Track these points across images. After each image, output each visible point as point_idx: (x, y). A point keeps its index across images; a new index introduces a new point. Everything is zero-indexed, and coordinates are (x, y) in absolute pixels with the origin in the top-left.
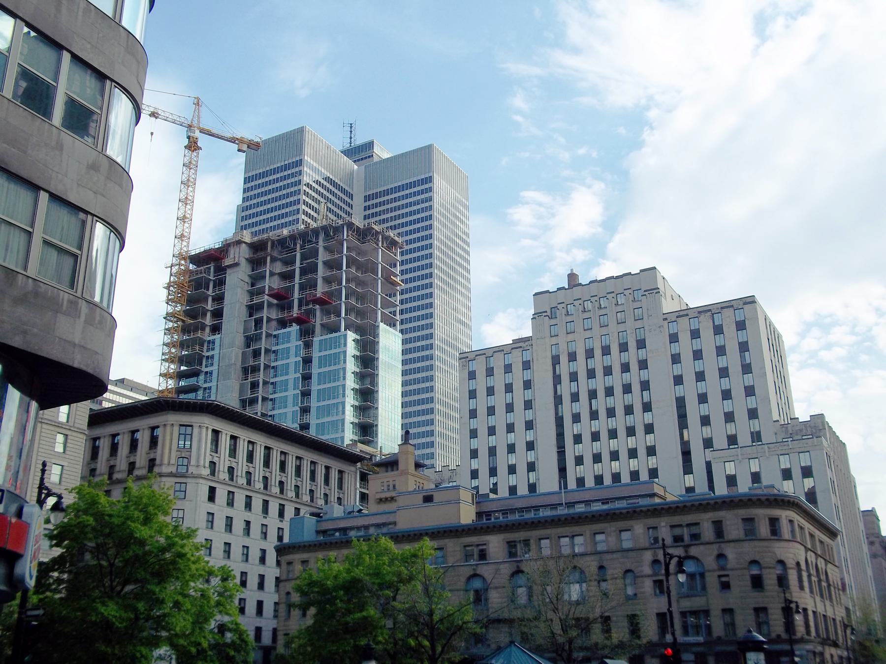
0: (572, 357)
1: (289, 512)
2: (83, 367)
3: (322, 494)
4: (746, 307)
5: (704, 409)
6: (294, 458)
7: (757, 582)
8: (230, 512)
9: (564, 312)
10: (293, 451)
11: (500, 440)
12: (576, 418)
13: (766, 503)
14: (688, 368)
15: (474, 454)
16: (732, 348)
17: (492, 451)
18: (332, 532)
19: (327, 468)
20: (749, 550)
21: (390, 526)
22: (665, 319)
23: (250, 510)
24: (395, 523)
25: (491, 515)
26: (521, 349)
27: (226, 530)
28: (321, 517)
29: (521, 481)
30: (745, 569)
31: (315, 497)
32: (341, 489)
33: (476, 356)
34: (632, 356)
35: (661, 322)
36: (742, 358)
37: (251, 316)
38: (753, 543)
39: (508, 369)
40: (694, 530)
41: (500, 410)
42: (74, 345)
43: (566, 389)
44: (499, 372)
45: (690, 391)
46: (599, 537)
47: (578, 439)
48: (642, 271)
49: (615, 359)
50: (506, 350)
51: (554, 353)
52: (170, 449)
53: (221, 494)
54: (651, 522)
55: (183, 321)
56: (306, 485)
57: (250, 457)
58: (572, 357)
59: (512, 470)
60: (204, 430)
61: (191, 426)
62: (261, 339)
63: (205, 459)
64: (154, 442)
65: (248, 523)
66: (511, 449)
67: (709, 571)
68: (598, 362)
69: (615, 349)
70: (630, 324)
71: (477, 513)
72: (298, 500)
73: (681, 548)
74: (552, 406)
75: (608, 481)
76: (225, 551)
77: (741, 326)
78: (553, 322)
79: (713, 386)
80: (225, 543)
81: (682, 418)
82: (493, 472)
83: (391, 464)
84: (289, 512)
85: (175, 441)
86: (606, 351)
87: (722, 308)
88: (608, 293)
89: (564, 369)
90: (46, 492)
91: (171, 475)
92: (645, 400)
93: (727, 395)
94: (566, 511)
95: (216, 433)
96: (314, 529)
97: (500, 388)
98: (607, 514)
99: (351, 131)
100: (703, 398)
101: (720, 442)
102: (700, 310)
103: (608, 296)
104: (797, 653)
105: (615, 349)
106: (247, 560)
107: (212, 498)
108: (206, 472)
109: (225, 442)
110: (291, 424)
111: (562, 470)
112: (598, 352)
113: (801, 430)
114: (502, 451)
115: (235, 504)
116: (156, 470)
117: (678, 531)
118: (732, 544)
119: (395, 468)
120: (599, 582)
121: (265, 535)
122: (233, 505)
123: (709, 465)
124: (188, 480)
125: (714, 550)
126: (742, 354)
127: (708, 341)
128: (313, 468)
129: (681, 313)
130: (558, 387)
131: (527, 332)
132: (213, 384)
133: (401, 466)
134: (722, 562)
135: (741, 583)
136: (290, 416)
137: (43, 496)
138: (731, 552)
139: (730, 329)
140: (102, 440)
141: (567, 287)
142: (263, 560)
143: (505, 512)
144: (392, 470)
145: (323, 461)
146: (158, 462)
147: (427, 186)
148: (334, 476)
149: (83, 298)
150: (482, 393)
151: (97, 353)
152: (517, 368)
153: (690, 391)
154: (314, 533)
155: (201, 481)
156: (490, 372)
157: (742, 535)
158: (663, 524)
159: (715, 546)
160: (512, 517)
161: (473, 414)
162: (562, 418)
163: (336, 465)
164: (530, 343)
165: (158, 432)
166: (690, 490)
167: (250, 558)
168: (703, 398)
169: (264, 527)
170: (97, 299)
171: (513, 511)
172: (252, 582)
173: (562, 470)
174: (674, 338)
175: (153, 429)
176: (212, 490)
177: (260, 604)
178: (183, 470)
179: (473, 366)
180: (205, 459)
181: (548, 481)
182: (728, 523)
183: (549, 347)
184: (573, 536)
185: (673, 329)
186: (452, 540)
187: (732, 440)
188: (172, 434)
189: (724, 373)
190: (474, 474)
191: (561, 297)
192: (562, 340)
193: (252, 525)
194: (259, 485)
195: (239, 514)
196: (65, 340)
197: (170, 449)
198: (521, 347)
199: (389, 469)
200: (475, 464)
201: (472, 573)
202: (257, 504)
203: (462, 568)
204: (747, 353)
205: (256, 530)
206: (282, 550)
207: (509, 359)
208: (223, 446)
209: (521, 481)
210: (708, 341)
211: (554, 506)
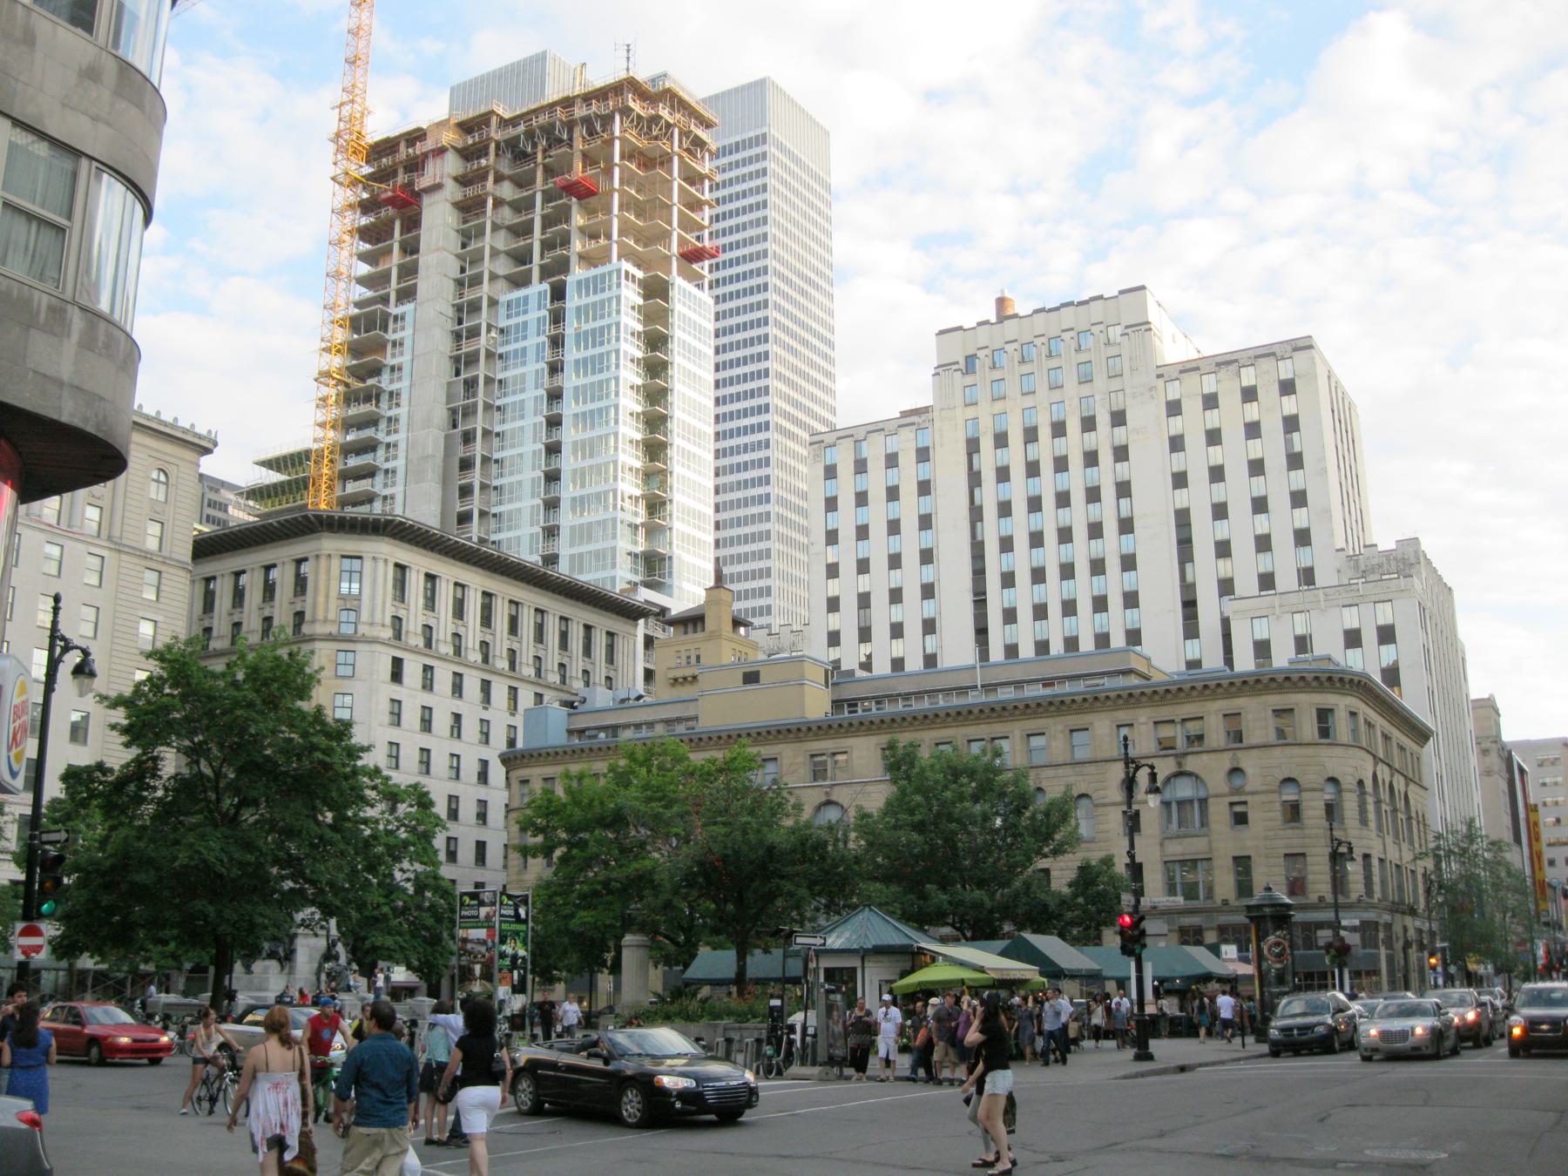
0: (1001, 440)
1: (526, 698)
2: (77, 422)
4: (1298, 356)
5: (1222, 530)
6: (532, 611)
7: (1294, 812)
9: (988, 362)
10: (531, 598)
11: (878, 582)
12: (1006, 544)
13: (1315, 684)
16: (1272, 428)
17: (864, 601)
18: (593, 733)
19: (588, 628)
20: (1284, 761)
21: (690, 724)
22: (1160, 376)
23: (461, 696)
24: (696, 718)
25: (856, 705)
26: (914, 428)
28: (575, 708)
29: (911, 650)
30: (1274, 792)
31: (568, 675)
33: (839, 438)
34: (1103, 439)
36: (1289, 443)
37: (458, 373)
38: (1287, 750)
39: (892, 460)
40: (1193, 728)
41: (878, 530)
42: (60, 383)
43: (989, 495)
44: (876, 465)
45: (1198, 497)
47: (1008, 580)
48: (1121, 292)
49: (1074, 445)
50: (892, 426)
51: (970, 434)
52: (327, 596)
53: (412, 670)
54: (1123, 716)
55: (347, 385)
56: (553, 657)
57: (459, 611)
58: (1001, 440)
59: (897, 631)
60: (381, 564)
61: (360, 558)
62: (475, 412)
63: (383, 612)
64: (301, 584)
65: (457, 717)
66: (896, 596)
67: (1217, 796)
68: (1045, 450)
69: (1073, 426)
70: (1100, 382)
71: (833, 702)
72: (540, 681)
73: (1171, 759)
75: (1057, 648)
76: (421, 762)
78: (969, 380)
79: (1238, 488)
80: (422, 750)
81: (1185, 544)
82: (865, 635)
83: (693, 621)
84: (526, 698)
85: (334, 583)
86: (1059, 429)
87: (1257, 357)
88: (1063, 331)
89: (987, 460)
90: (62, 644)
91: (330, 638)
92: (1124, 514)
93: (1260, 505)
94: (983, 699)
95: (401, 568)
96: (565, 727)
97: (877, 494)
98: (1051, 703)
99: (628, 58)
100: (1220, 511)
101: (1246, 584)
102: (1219, 360)
104: (1344, 923)
105: (1073, 426)
106: (458, 777)
107: (397, 676)
108: (387, 633)
109: (416, 583)
110: (530, 556)
111: (982, 632)
112: (1045, 433)
113: (1380, 566)
114: (880, 600)
116: (306, 629)
117: (1166, 732)
118: (1255, 752)
121: (486, 737)
122: (431, 689)
123: (1226, 623)
124: (359, 647)
125: (1225, 762)
126: (1289, 436)
128: (564, 629)
129: (1189, 366)
130: (977, 491)
132: (398, 490)
133: (710, 623)
134: (1237, 782)
135: (1264, 816)
137: (58, 650)
138: (1251, 763)
140: (219, 581)
141: (993, 320)
142: (483, 777)
143: (879, 701)
144: (695, 631)
145: (581, 615)
146: (308, 617)
148: (600, 641)
149: (74, 303)
150: (846, 501)
151: (101, 399)
152: (907, 459)
153: (1198, 497)
154: (565, 734)
155: (378, 648)
156: (861, 467)
157: (1272, 737)
158: (1142, 720)
159: (1229, 754)
160: (889, 708)
162: (982, 543)
163: (603, 622)
164: (930, 416)
166: (1194, 664)
167: (462, 774)
168: (1220, 511)
169: (485, 724)
170: (104, 306)
171: (893, 698)
172: (468, 811)
173: (982, 632)
176: (397, 663)
177: (481, 847)
178: (348, 630)
179: (832, 456)
180: (383, 612)
181: (957, 649)
182: (1250, 717)
183: (961, 423)
185: (1174, 392)
186: (791, 745)
187: (1267, 581)
188: (329, 571)
189: (1257, 467)
190: (834, 639)
191: (983, 337)
193: (464, 721)
194: (475, 657)
195: (443, 705)
196: (45, 376)
197: (327, 596)
199: (690, 627)
200: (835, 622)
201: (824, 799)
202: (472, 685)
203: (809, 790)
204: (1296, 435)
205: (470, 728)
206: (510, 760)
207: (893, 445)
208: (413, 590)
209: (911, 650)
211: (962, 690)
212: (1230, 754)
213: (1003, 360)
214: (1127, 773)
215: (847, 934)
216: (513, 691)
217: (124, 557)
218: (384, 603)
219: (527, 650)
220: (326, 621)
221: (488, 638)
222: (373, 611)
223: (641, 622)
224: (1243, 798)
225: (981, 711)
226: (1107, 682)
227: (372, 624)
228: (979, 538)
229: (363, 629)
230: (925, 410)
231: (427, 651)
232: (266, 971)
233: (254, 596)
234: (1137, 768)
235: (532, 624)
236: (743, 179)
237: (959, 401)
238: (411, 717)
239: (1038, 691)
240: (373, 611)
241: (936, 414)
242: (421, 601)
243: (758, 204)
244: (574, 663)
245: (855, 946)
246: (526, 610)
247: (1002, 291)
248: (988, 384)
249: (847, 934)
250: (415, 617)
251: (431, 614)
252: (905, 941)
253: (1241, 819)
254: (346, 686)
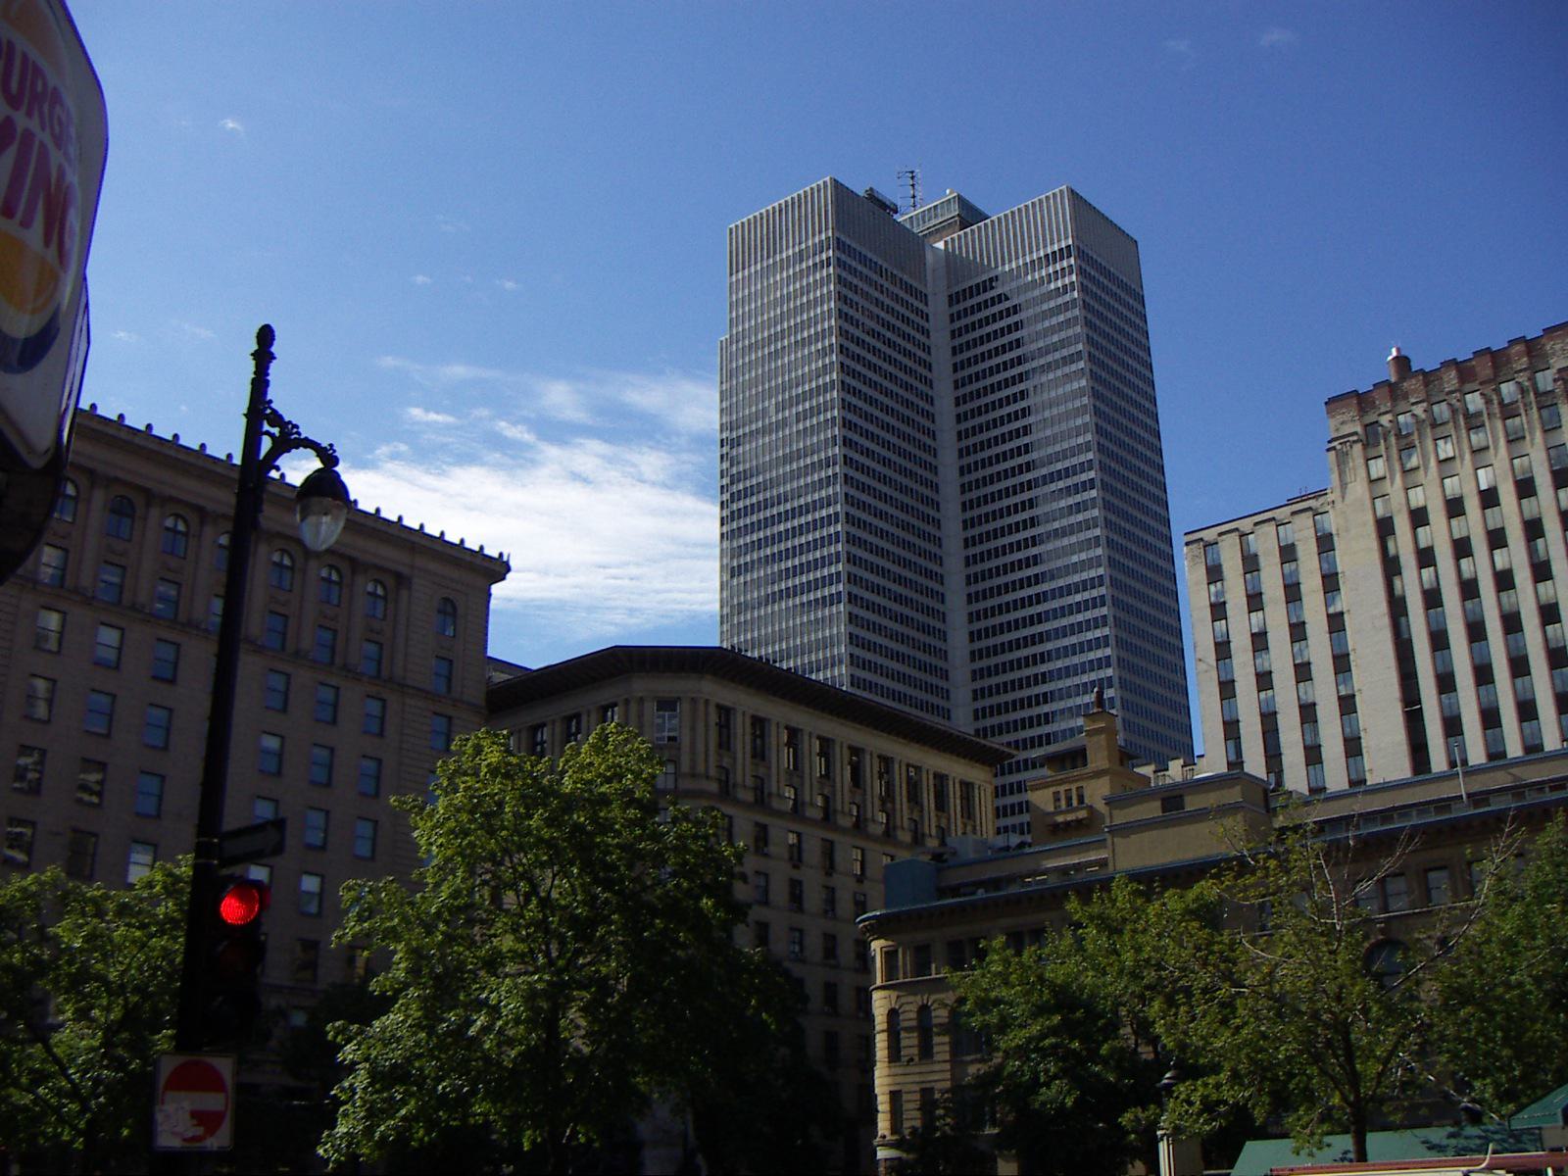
0: (1419, 517)
26: (1310, 513)
28: (946, 861)
63: (706, 761)
74: (1385, 621)
89: (1403, 544)
90: (276, 431)
119: (1079, 762)
130: (1397, 582)
137: (266, 444)
180: (706, 761)
198: (1310, 509)
222: (693, 761)
227: (694, 775)
228: (1406, 636)
240: (693, 761)
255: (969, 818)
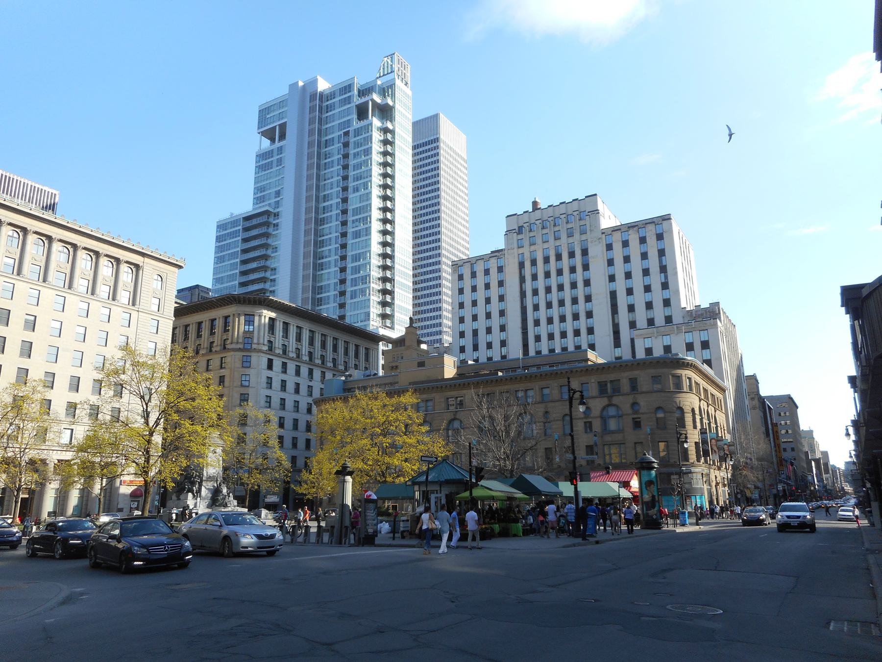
0: (534, 262)
3: (342, 362)
4: (665, 223)
5: (631, 300)
6: (332, 339)
8: (284, 377)
9: (528, 228)
10: (331, 334)
11: (481, 325)
14: (619, 269)
15: (462, 335)
17: (475, 333)
19: (357, 346)
22: (603, 233)
27: (281, 390)
32: (358, 358)
35: (600, 235)
36: (660, 261)
39: (487, 272)
43: (529, 286)
45: (620, 285)
46: (546, 391)
47: (537, 323)
48: (586, 197)
50: (486, 258)
53: (277, 364)
58: (534, 262)
59: (489, 346)
61: (254, 315)
63: (264, 339)
66: (489, 331)
67: (627, 415)
70: (577, 236)
73: (606, 398)
74: (518, 299)
77: (660, 237)
78: (520, 237)
79: (638, 282)
82: (476, 348)
84: (329, 375)
86: (559, 257)
87: (646, 224)
89: (528, 271)
98: (551, 374)
100: (630, 292)
101: (642, 322)
102: (629, 225)
103: (561, 216)
106: (298, 411)
107: (270, 366)
108: (265, 348)
111: (525, 346)
112: (553, 259)
113: (702, 314)
114: (482, 333)
115: (288, 371)
120: (544, 423)
121: (310, 394)
123: (632, 340)
124: (253, 354)
125: (630, 399)
127: (635, 250)
129: (616, 229)
130: (523, 285)
131: (502, 246)
133: (407, 343)
134: (636, 408)
136: (331, 310)
139: (651, 240)
140: (191, 326)
141: (531, 210)
142: (309, 411)
144: (401, 346)
145: (353, 341)
147: (435, 145)
148: (362, 352)
152: (494, 272)
153: (620, 285)
155: (262, 354)
156: (474, 275)
161: (461, 305)
163: (363, 344)
165: (230, 319)
166: (617, 358)
167: (300, 409)
168: (630, 292)
173: (525, 346)
174: (609, 247)
175: (226, 318)
180: (264, 339)
181: (515, 351)
183: (516, 255)
184: (527, 390)
187: (651, 322)
191: (526, 218)
192: (526, 251)
193: (300, 386)
194: (306, 358)
195: (291, 380)
199: (399, 344)
200: (462, 342)
202: (304, 370)
203: (446, 414)
205: (303, 390)
208: (278, 329)
210: (635, 250)
211: (514, 369)
212: (633, 396)
213: (534, 227)
214: (569, 395)
215: (434, 474)
216: (323, 373)
217: (140, 313)
218: (264, 335)
219: (330, 355)
220: (237, 343)
221: (312, 350)
222: (259, 338)
223: (381, 343)
224: (639, 416)
225: (521, 378)
226: (577, 365)
227: (258, 344)
229: (254, 346)
230: (501, 250)
231: (284, 356)
232: (186, 498)
233: (205, 332)
234: (574, 393)
235: (332, 344)
236: (429, 157)
237: (516, 245)
238: (276, 384)
239: (547, 368)
240: (259, 338)
241: (506, 251)
242: (281, 334)
243: (435, 168)
244: (351, 361)
245: (436, 480)
246: (329, 338)
247: (535, 198)
248: (528, 238)
249: (434, 474)
250: (278, 341)
251: (286, 340)
252: (461, 477)
253: (637, 424)
254: (247, 371)
255: (368, 361)
